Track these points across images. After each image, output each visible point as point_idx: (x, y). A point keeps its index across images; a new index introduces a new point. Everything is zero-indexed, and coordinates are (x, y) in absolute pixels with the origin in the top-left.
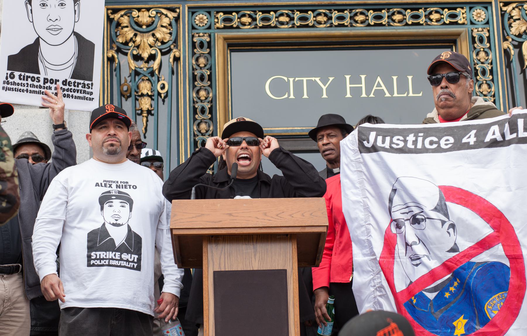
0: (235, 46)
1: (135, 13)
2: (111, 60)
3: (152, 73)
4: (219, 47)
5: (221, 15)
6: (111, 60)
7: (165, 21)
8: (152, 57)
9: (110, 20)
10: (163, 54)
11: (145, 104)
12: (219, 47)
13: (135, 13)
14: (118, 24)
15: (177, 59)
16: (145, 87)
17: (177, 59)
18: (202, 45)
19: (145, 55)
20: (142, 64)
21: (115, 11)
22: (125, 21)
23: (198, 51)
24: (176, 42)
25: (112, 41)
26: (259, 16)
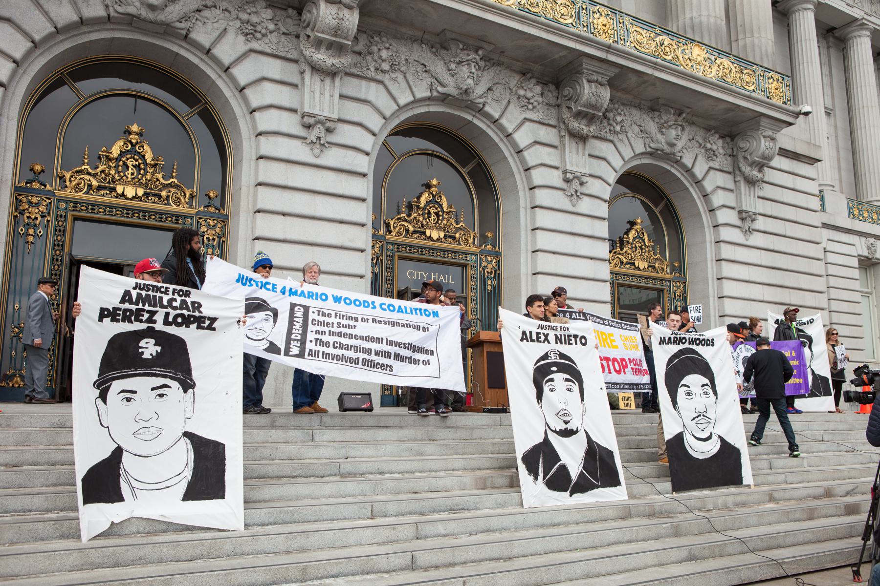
0: (76, 218)
1: (30, 197)
2: (16, 217)
3: (36, 225)
4: (70, 219)
5: (72, 205)
6: (16, 217)
7: (45, 203)
8: (36, 218)
9: (17, 199)
10: (42, 217)
11: (31, 239)
12: (70, 219)
13: (30, 197)
14: (21, 201)
15: (48, 221)
16: (31, 231)
17: (48, 221)
18: (61, 216)
19: (33, 217)
20: (32, 222)
21: (20, 195)
22: (24, 200)
23: (59, 218)
24: (49, 213)
25: (17, 209)
26: (90, 207)
